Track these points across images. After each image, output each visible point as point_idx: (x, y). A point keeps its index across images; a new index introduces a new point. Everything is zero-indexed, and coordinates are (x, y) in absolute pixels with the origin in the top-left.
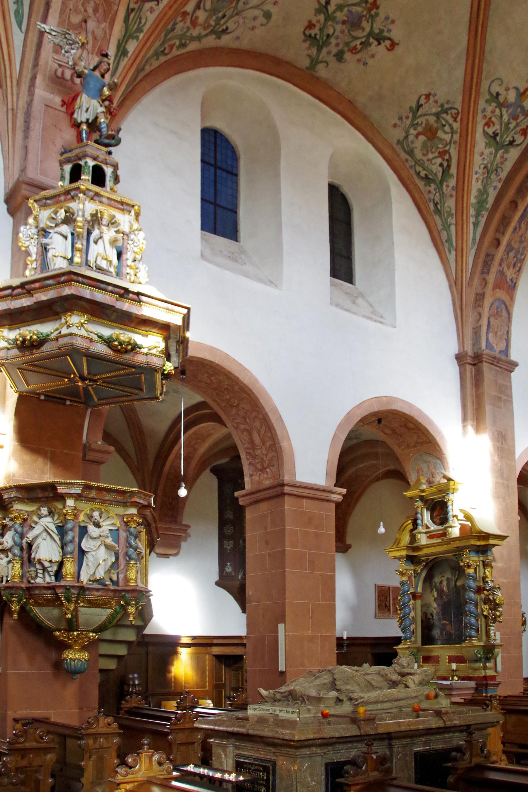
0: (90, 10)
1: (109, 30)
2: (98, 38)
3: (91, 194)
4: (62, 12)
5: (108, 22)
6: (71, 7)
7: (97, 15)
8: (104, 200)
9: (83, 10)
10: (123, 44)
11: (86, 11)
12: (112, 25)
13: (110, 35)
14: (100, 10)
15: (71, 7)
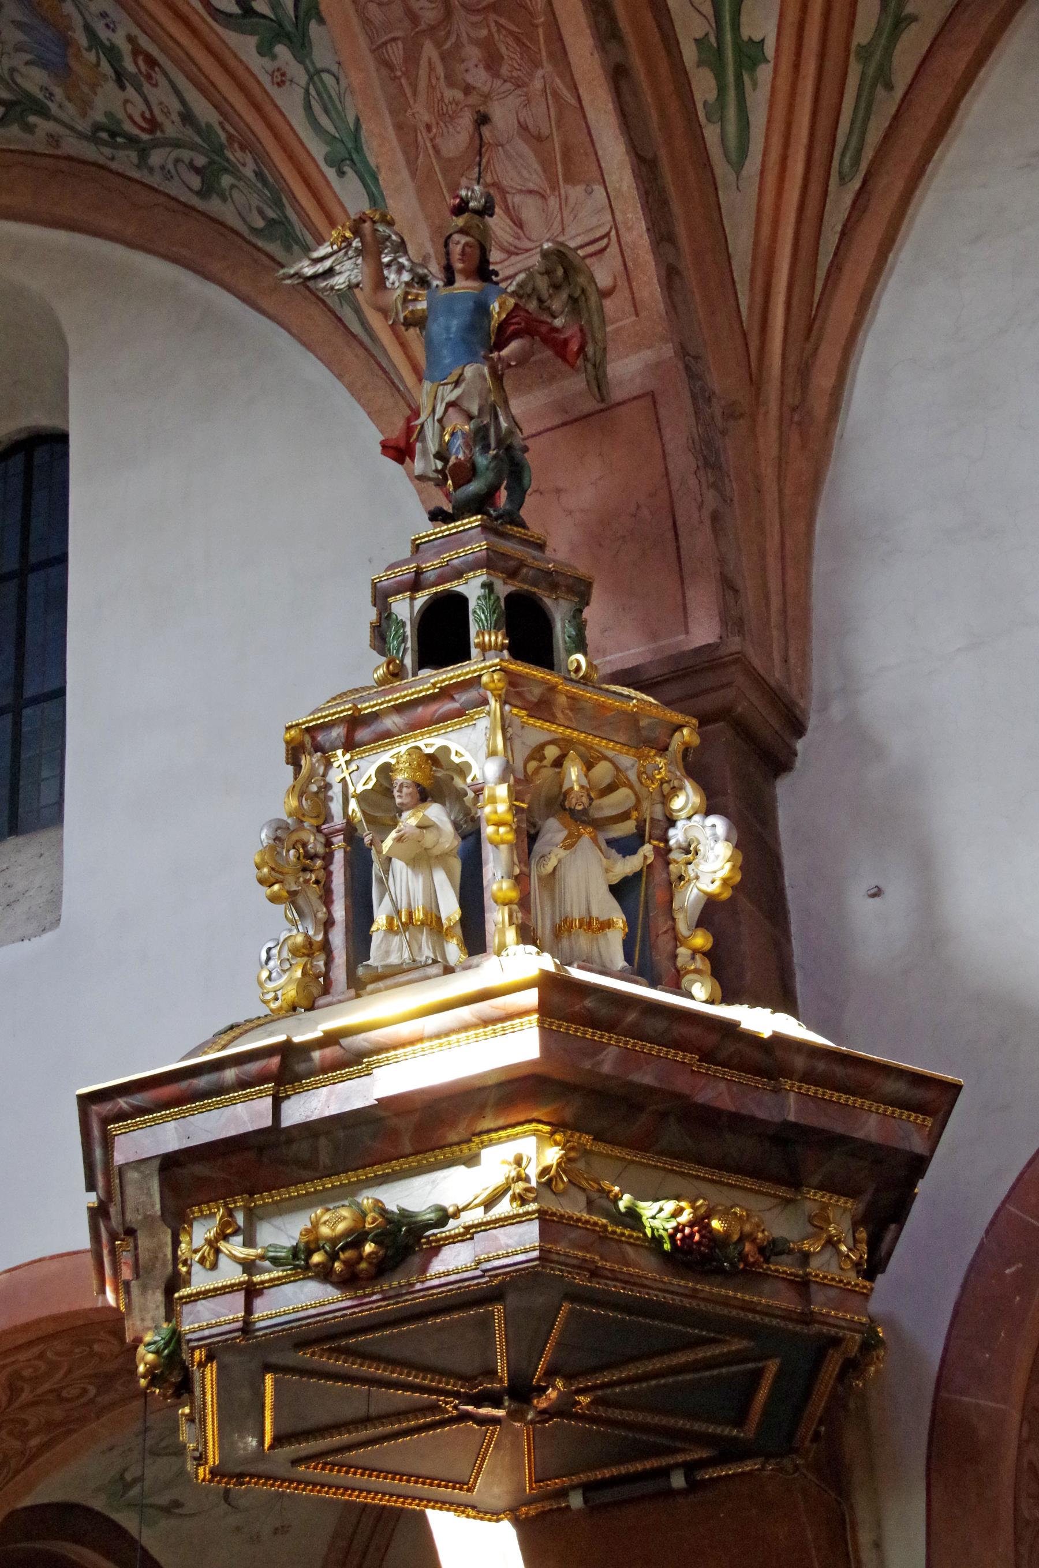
0: (479, 77)
1: (561, 76)
2: (545, 132)
3: (338, 733)
4: (411, 149)
5: (545, 64)
6: (426, 118)
7: (504, 70)
8: (391, 722)
9: (459, 95)
10: (728, 37)
11: (468, 90)
12: (561, 56)
13: (575, 88)
14: (506, 48)
15: (426, 118)
